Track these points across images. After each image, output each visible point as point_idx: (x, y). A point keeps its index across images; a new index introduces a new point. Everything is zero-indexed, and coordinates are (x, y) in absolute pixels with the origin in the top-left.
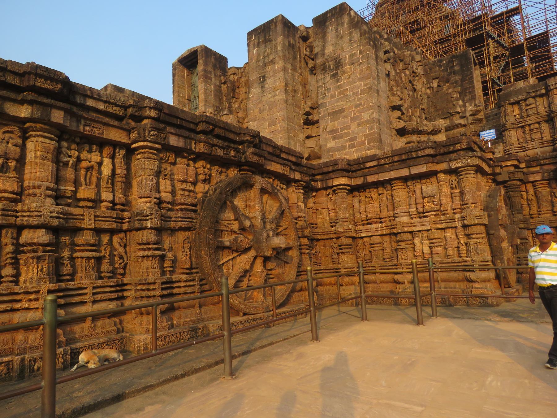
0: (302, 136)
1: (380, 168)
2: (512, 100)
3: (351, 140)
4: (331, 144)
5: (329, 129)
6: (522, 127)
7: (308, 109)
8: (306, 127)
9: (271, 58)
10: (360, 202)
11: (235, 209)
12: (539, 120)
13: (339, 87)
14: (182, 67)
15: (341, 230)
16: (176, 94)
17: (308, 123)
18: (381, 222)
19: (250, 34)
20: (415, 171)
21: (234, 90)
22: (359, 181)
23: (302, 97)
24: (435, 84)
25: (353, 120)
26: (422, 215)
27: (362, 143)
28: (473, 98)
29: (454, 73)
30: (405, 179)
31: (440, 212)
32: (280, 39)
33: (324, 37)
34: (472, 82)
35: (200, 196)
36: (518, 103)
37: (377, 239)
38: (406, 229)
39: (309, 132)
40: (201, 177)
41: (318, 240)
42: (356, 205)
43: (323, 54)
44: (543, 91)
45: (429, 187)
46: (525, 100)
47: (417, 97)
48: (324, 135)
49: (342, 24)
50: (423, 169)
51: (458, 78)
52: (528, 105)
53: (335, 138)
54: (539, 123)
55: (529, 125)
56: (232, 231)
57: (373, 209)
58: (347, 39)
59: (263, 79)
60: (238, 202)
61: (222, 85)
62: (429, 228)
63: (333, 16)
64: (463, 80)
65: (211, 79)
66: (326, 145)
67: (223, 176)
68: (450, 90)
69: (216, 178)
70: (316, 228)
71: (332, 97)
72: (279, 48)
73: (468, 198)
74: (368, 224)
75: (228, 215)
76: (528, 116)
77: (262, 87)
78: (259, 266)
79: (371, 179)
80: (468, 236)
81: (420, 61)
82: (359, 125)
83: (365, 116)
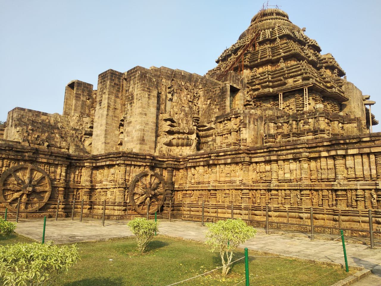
0: (117, 132)
2: (219, 121)
6: (222, 135)
7: (122, 118)
8: (121, 127)
11: (16, 176)
12: (227, 133)
14: (70, 89)
15: (84, 185)
16: (65, 103)
17: (122, 125)
18: (101, 183)
19: (99, 75)
23: (121, 111)
24: (208, 103)
25: (134, 128)
26: (110, 181)
27: (135, 140)
32: (108, 82)
35: (3, 172)
38: (104, 187)
39: (122, 130)
40: (5, 165)
41: (80, 189)
44: (229, 118)
45: (112, 170)
46: (224, 121)
47: (195, 110)
52: (225, 124)
54: (227, 134)
55: (224, 135)
56: (14, 184)
58: (136, 85)
60: (19, 174)
61: (87, 100)
62: (110, 187)
65: (80, 98)
67: (16, 165)
68: (214, 107)
69: (12, 165)
70: (79, 183)
75: (13, 178)
76: (224, 130)
78: (24, 197)
81: (201, 88)
83: (138, 127)
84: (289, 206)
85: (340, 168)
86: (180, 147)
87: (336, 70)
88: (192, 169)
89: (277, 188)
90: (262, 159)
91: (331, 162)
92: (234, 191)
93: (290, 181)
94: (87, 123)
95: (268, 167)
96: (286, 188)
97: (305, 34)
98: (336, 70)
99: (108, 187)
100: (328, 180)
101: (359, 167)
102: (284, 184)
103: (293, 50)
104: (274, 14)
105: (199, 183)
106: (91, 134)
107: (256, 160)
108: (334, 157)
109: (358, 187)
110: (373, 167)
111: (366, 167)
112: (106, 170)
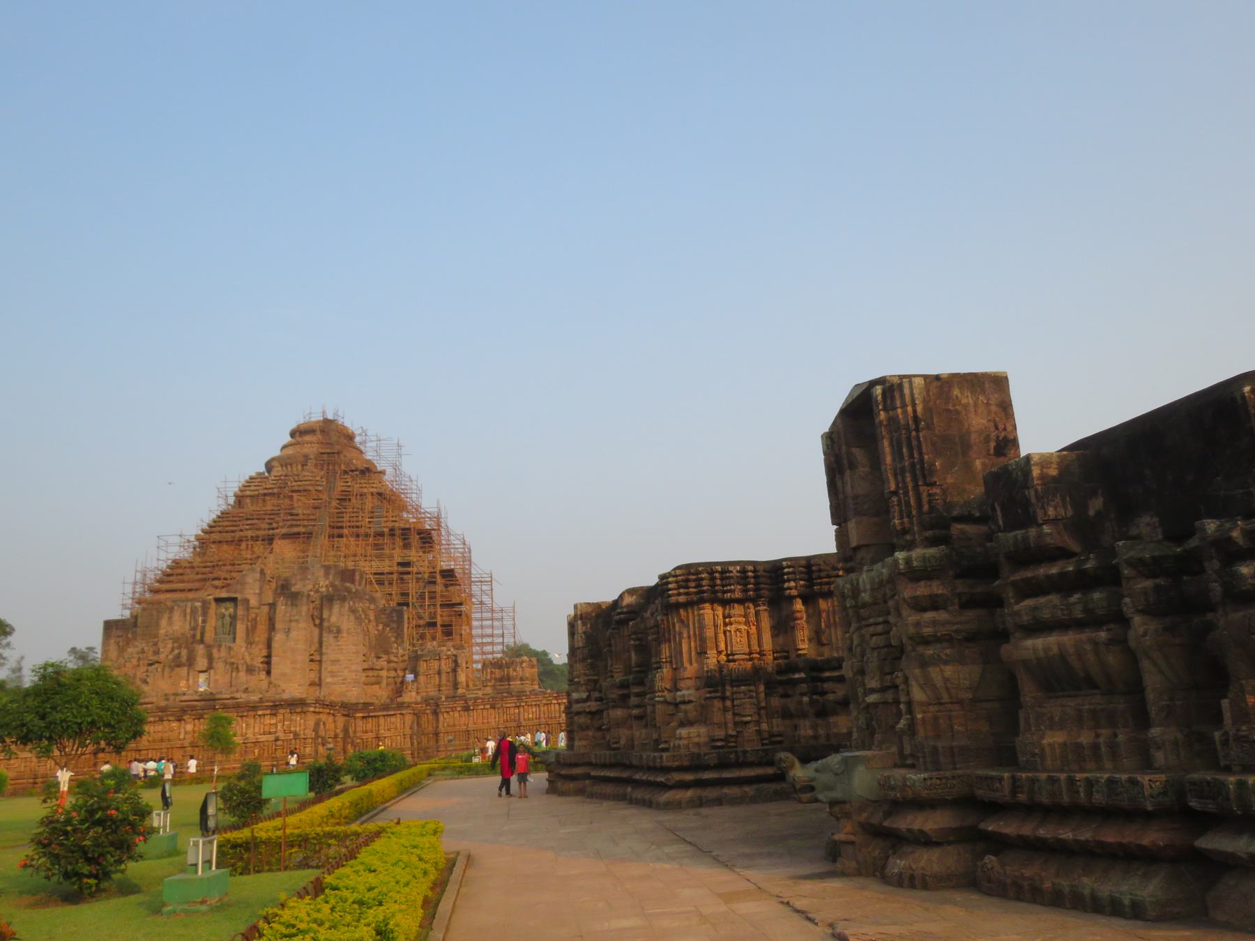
1: (374, 710)
4: (328, 680)
5: (329, 670)
7: (312, 652)
9: (296, 618)
13: (338, 645)
20: (389, 713)
21: (256, 627)
22: (366, 715)
24: (380, 627)
25: (345, 668)
26: (389, 730)
27: (350, 683)
28: (403, 642)
29: (393, 621)
30: (384, 716)
31: (396, 729)
33: (331, 609)
34: (402, 631)
36: (426, 661)
43: (329, 621)
45: (393, 719)
48: (324, 674)
49: (344, 607)
50: (393, 713)
51: (395, 625)
53: (332, 676)
57: (369, 726)
59: (288, 631)
63: (338, 599)
64: (398, 628)
68: (390, 635)
71: (333, 650)
72: (304, 614)
73: (406, 724)
77: (287, 636)
79: (371, 714)
82: (349, 672)
83: (354, 667)
86: (370, 686)
88: (445, 714)
90: (514, 705)
91: (557, 706)
92: (492, 731)
95: (517, 711)
107: (509, 705)
108: (559, 704)
112: (382, 720)
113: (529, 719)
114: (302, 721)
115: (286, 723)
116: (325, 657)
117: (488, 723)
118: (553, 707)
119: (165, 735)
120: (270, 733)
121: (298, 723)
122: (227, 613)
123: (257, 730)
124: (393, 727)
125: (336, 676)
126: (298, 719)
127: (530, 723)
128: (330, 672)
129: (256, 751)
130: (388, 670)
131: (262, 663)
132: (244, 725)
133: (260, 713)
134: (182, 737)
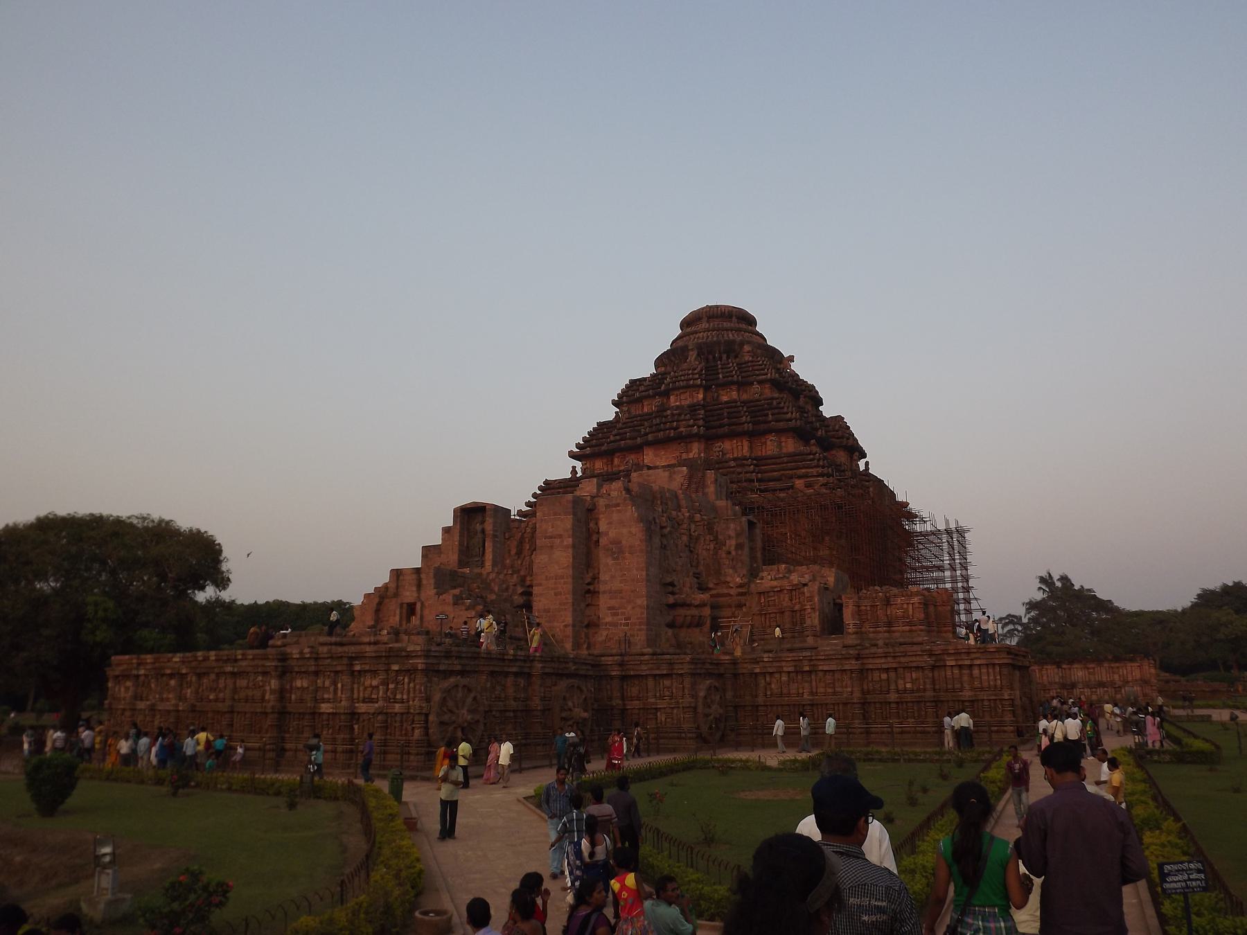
3: (626, 619)
4: (609, 619)
8: (587, 595)
10: (627, 685)
15: (615, 704)
24: (712, 546)
26: (662, 697)
37: (637, 711)
38: (653, 706)
42: (625, 687)
45: (667, 682)
55: (770, 613)
66: (604, 619)
74: (632, 700)
80: (684, 713)
82: (633, 608)
83: (639, 602)
84: (913, 720)
85: (965, 678)
87: (857, 454)
89: (899, 700)
91: (956, 671)
93: (912, 691)
94: (515, 585)
95: (884, 676)
96: (909, 700)
97: (794, 367)
98: (857, 454)
99: (659, 706)
100: (954, 690)
101: (985, 677)
102: (906, 695)
103: (794, 421)
104: (734, 318)
105: (781, 694)
106: (528, 606)
107: (871, 667)
109: (985, 698)
110: (998, 677)
111: (992, 678)
113: (905, 690)
114: (412, 685)
115: (391, 686)
116: (602, 588)
117: (834, 693)
118: (949, 673)
119: (250, 693)
120: (371, 701)
121: (406, 687)
122: (479, 527)
123: (355, 696)
124: (667, 693)
125: (616, 614)
126: (406, 680)
127: (908, 697)
128: (610, 608)
129: (356, 727)
130: (713, 607)
131: (522, 594)
132: (339, 685)
133: (358, 668)
134: (267, 697)
